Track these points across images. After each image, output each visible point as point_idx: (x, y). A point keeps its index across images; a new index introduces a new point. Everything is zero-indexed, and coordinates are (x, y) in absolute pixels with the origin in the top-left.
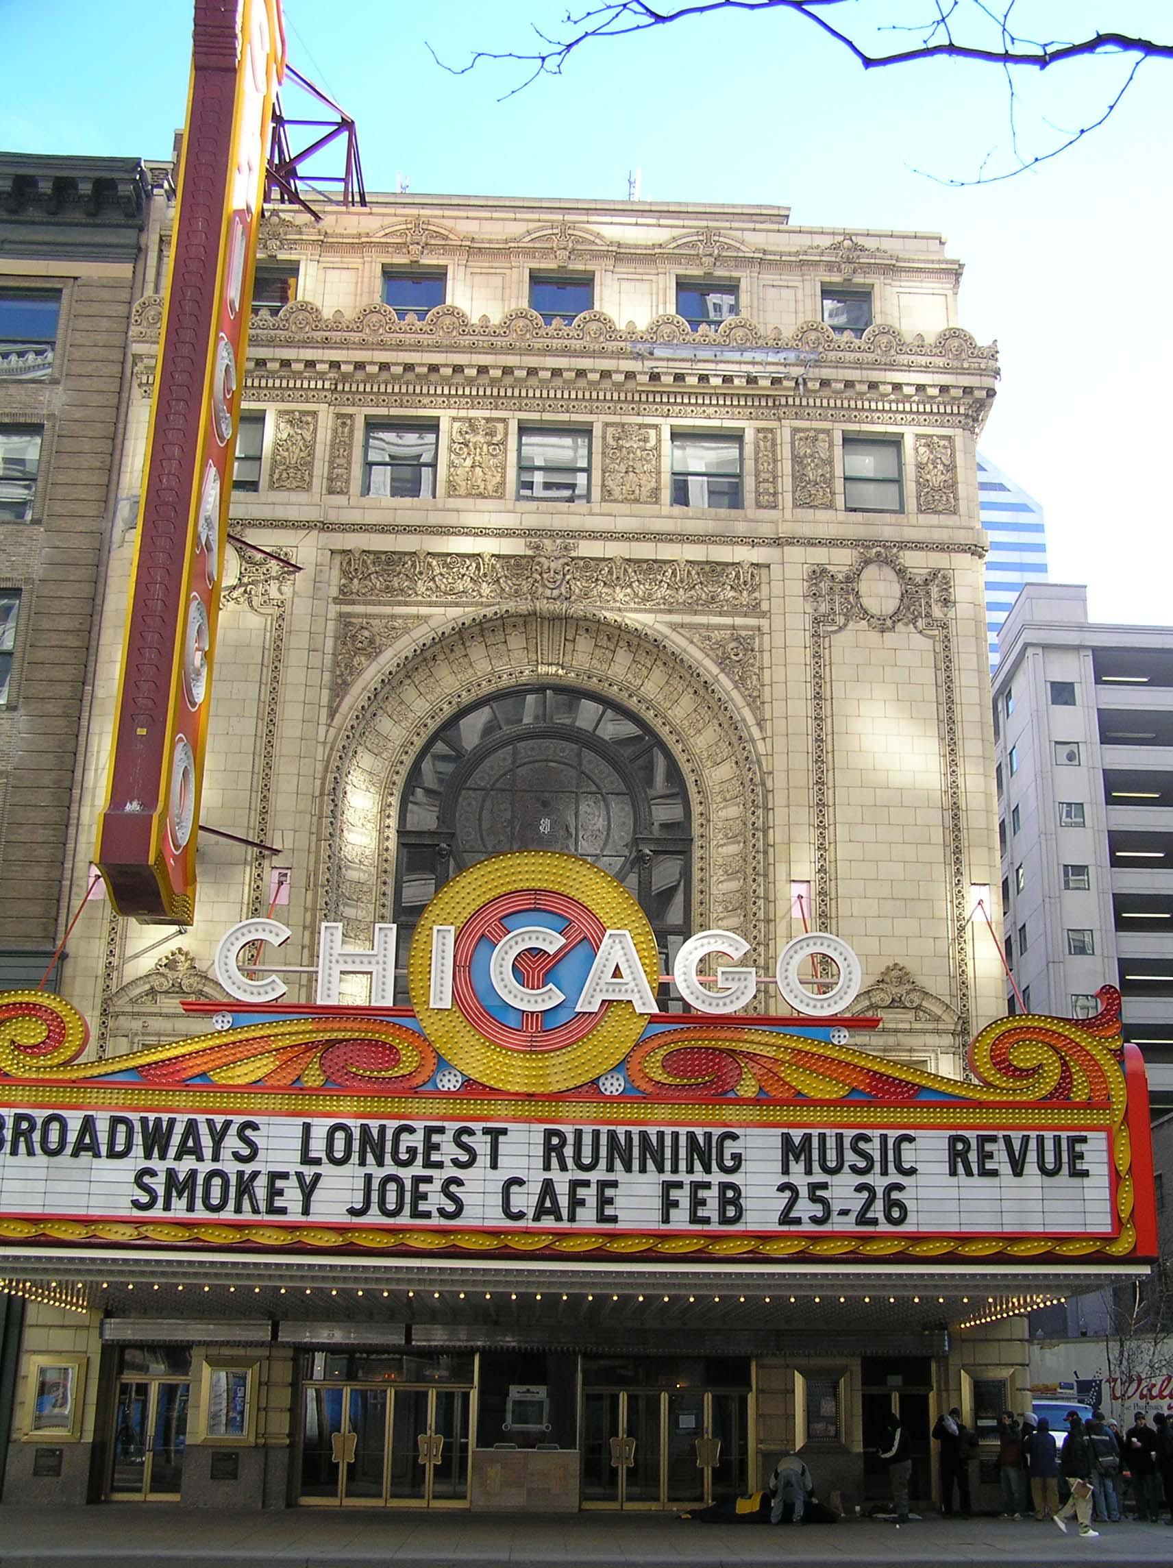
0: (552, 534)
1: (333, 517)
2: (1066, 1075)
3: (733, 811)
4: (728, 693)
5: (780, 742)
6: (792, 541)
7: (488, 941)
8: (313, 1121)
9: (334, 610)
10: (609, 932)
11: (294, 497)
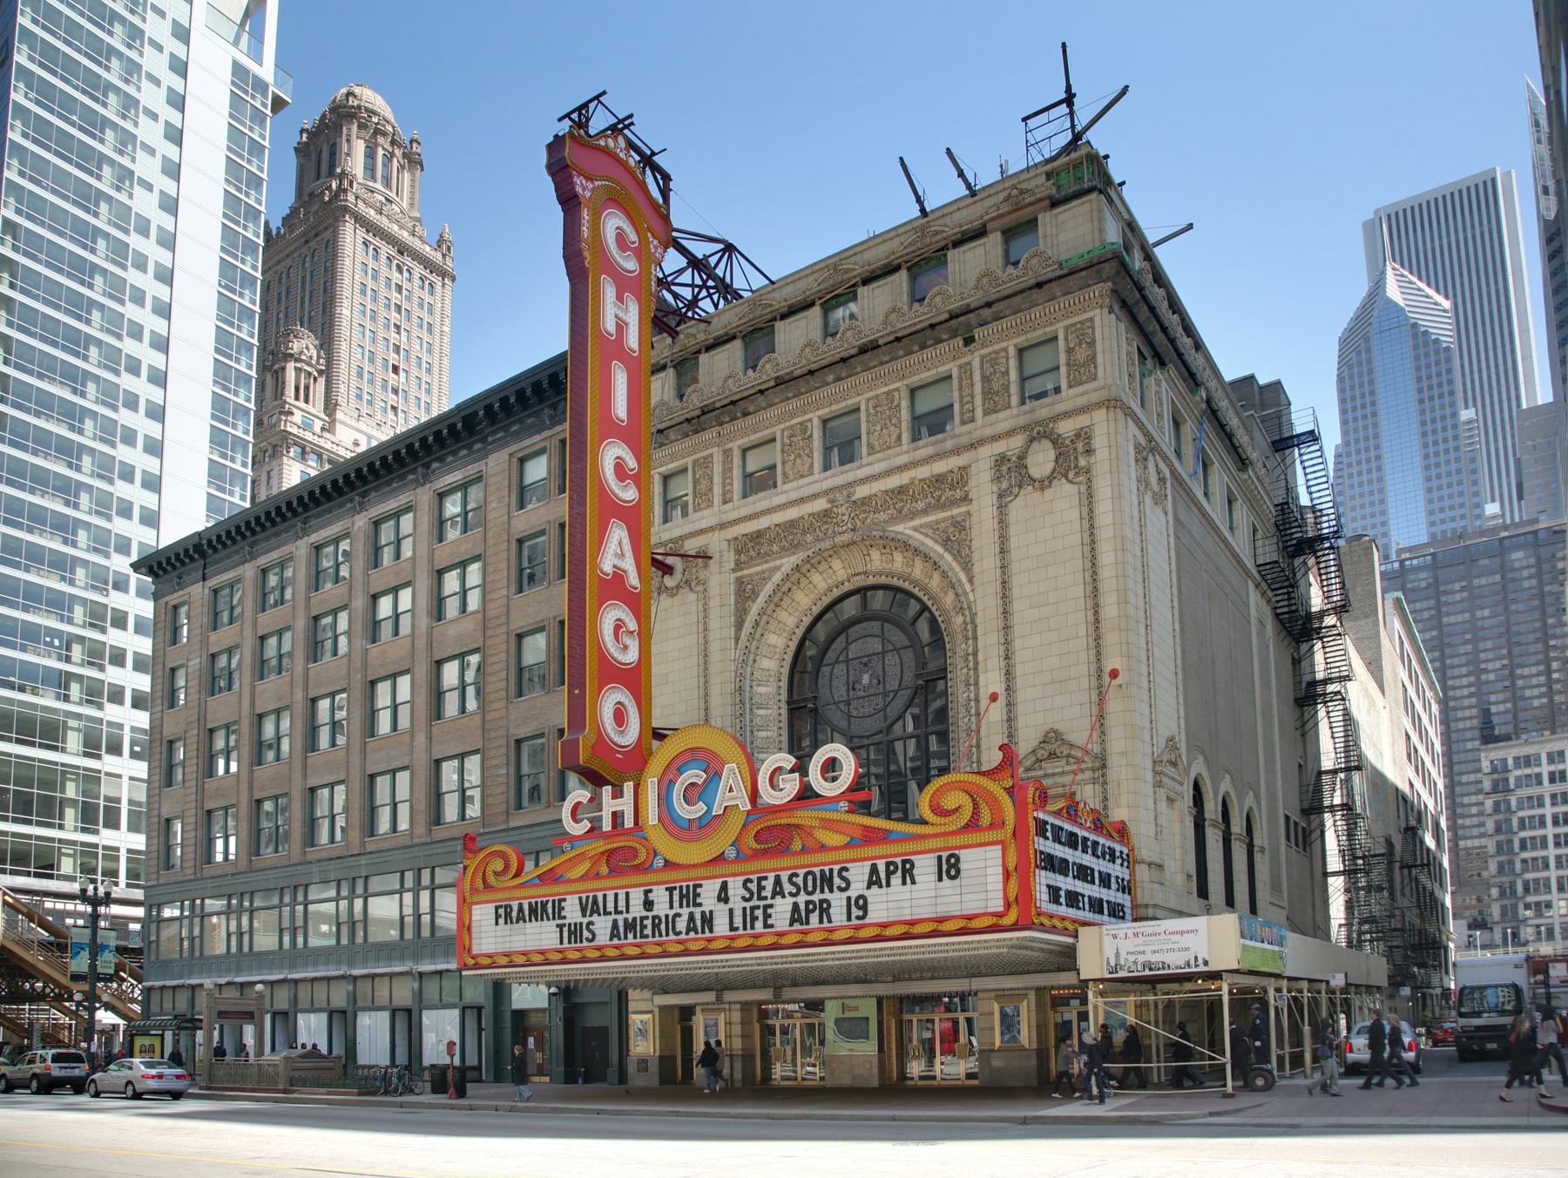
0: (839, 488)
1: (725, 519)
4: (949, 565)
5: (979, 590)
6: (973, 446)
9: (733, 576)
11: (705, 513)
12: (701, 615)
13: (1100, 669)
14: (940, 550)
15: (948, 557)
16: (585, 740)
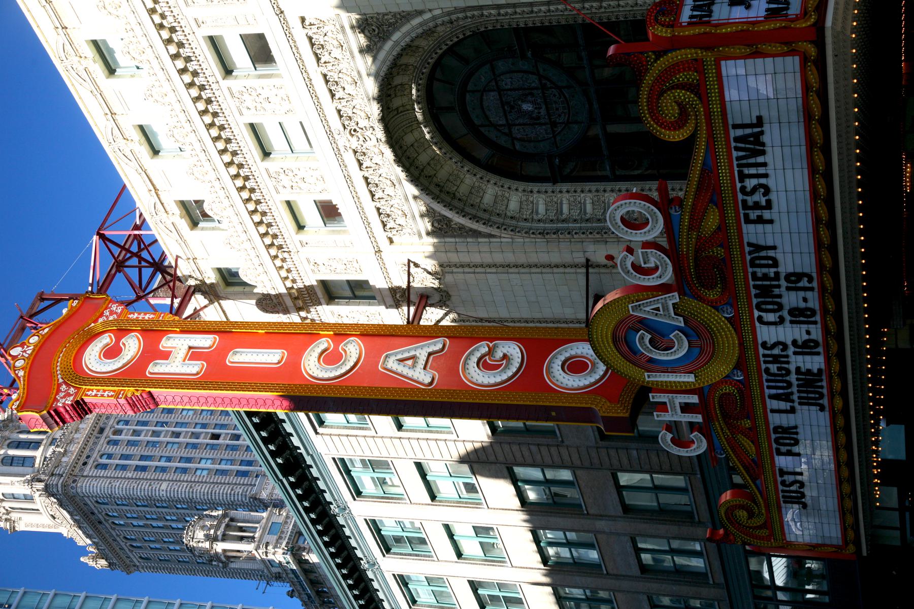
2: (682, 86)
5: (430, 6)
7: (651, 360)
8: (769, 407)
12: (467, 270)
14: (388, 45)
15: (396, 36)
16: (604, 408)
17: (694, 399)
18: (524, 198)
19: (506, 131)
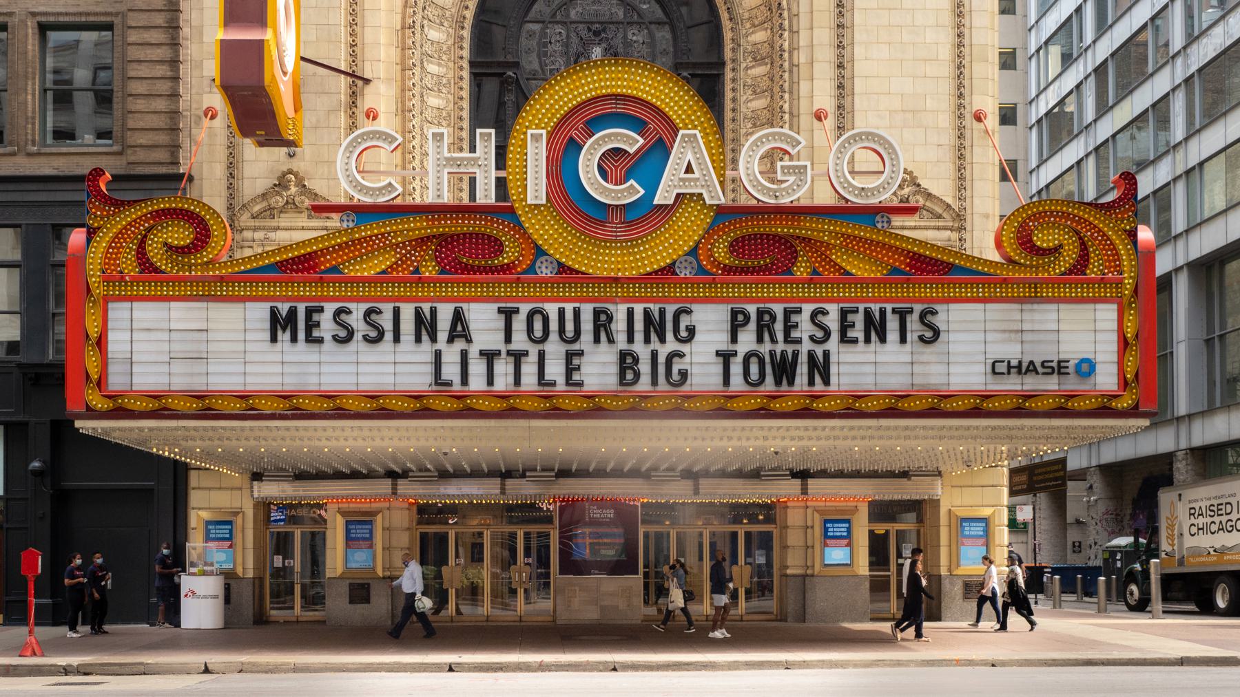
3: (760, 36)
7: (574, 147)
10: (681, 132)
13: (961, 106)
17: (486, 195)
18: (448, 14)
19: (558, 17)
